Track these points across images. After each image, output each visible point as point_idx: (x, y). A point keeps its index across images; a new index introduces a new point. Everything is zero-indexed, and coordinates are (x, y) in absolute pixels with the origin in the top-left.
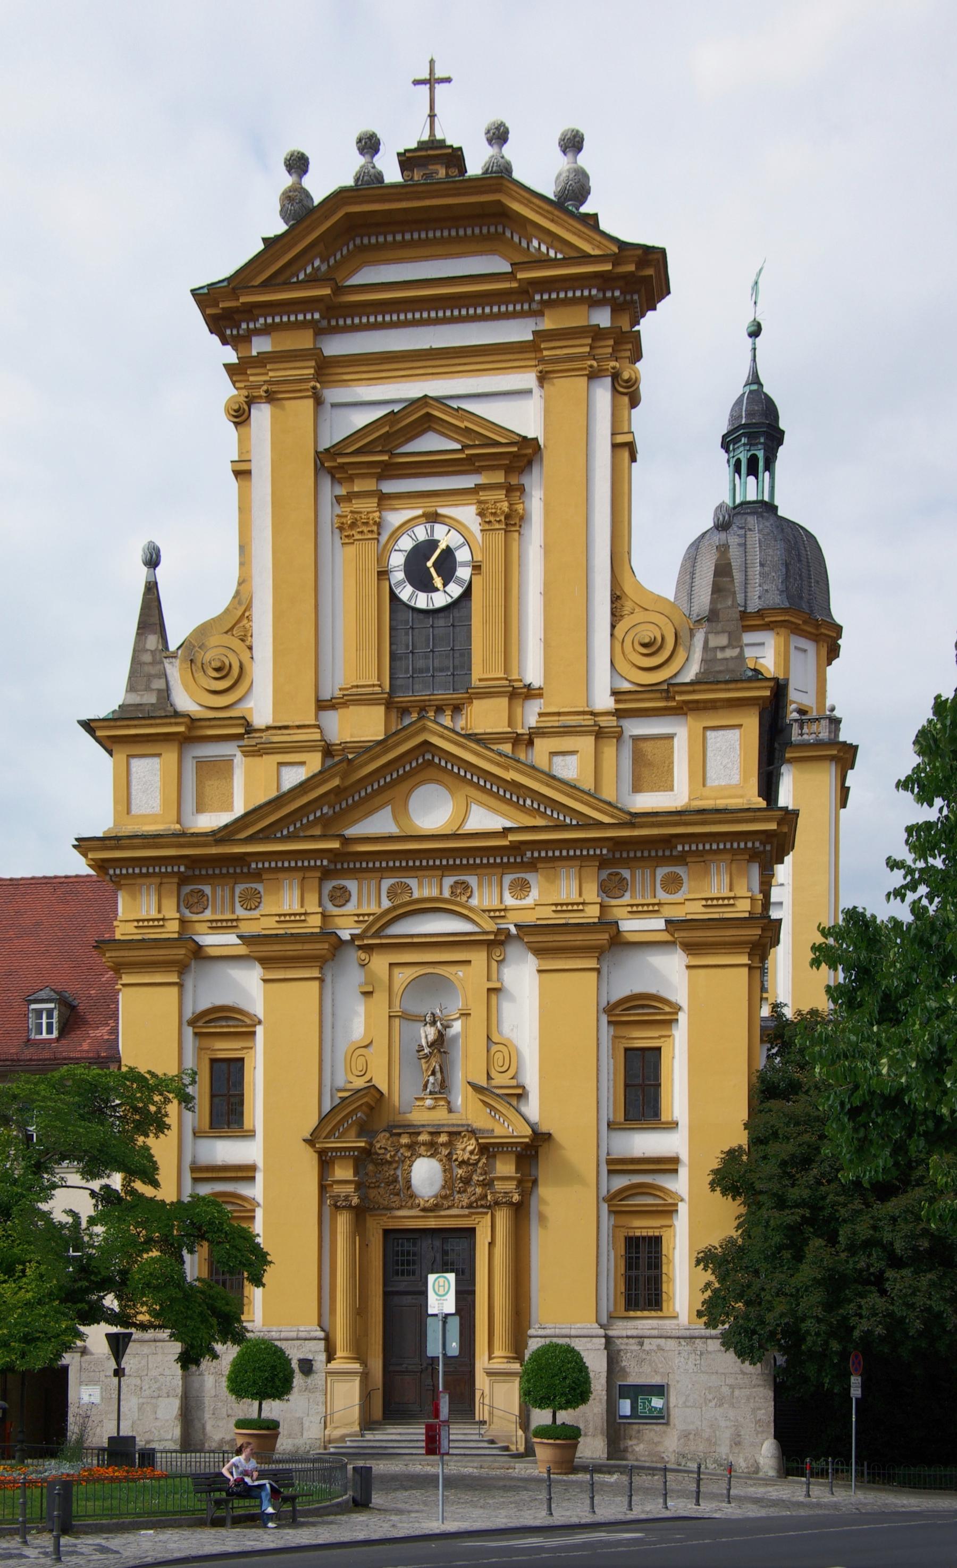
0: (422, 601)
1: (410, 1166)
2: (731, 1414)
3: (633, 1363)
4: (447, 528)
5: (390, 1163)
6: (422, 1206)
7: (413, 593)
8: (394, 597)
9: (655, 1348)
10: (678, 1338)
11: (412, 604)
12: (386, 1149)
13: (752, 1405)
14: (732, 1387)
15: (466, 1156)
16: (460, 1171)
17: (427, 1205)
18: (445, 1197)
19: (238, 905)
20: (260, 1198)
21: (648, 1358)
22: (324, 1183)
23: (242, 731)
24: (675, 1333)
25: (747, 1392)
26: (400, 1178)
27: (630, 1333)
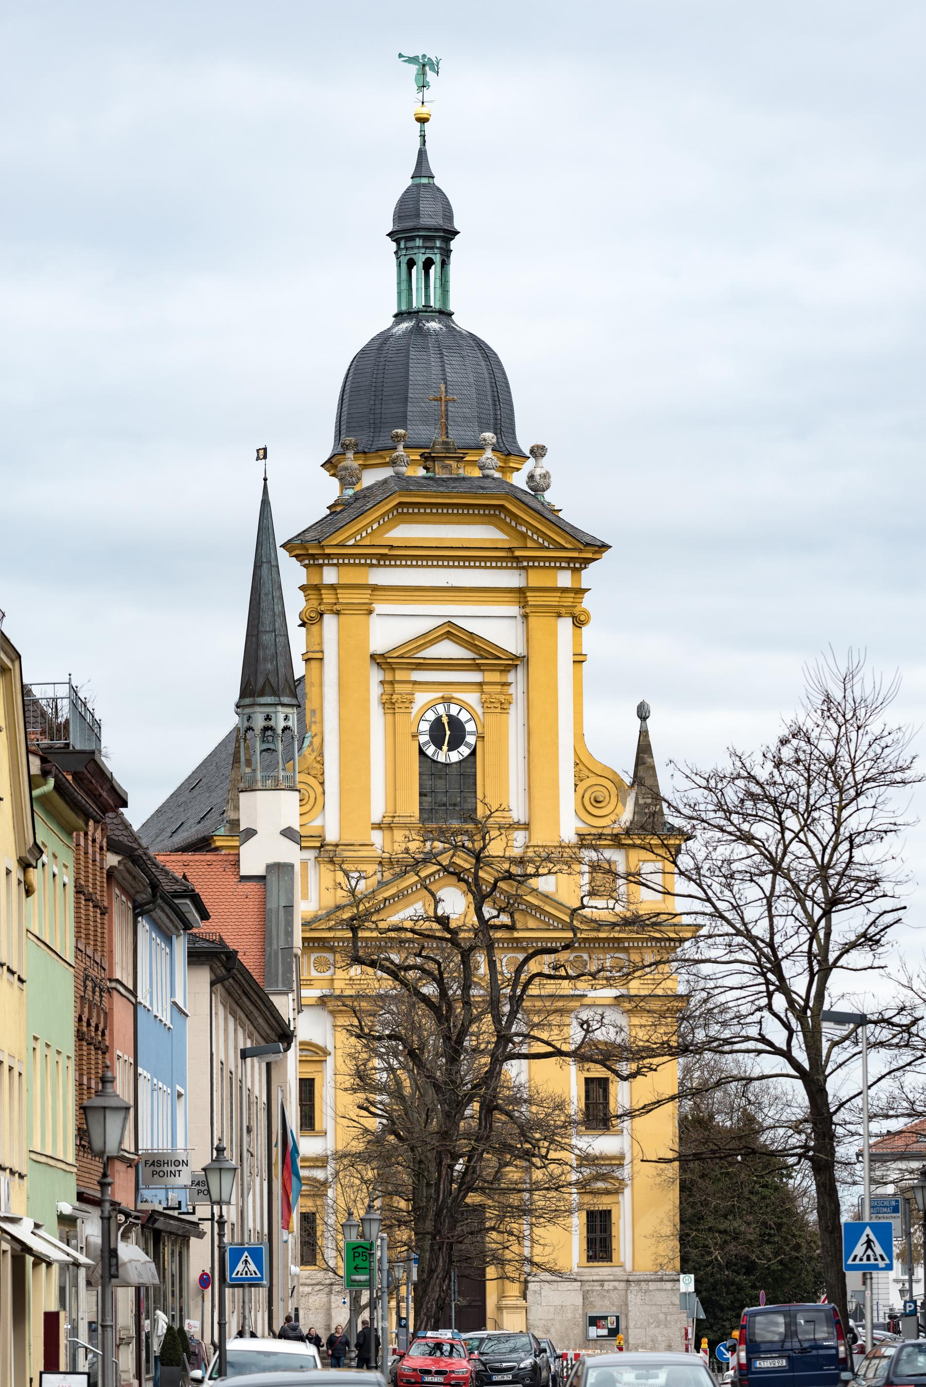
0: (441, 758)
2: (665, 1332)
4: (459, 708)
7: (436, 751)
8: (422, 753)
10: (628, 1281)
11: (435, 758)
13: (679, 1326)
14: (666, 1314)
19: (312, 968)
23: (318, 844)
24: (625, 1278)
25: (675, 1317)
27: (595, 1278)
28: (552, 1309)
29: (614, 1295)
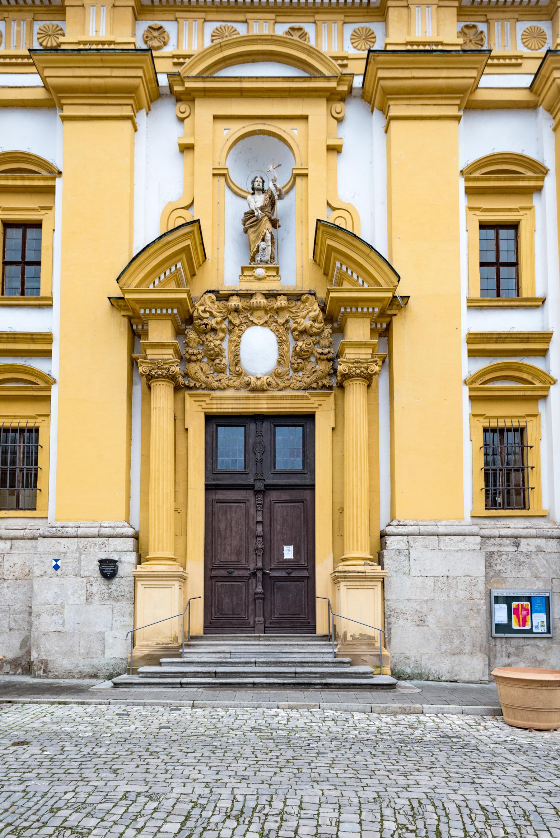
1: (240, 337)
3: (510, 567)
5: (214, 330)
6: (253, 384)
9: (534, 550)
12: (211, 313)
15: (307, 323)
16: (300, 343)
17: (259, 383)
18: (278, 375)
20: (55, 374)
21: (527, 561)
22: (135, 355)
26: (226, 353)
27: (504, 532)
28: (429, 582)
29: (539, 561)
